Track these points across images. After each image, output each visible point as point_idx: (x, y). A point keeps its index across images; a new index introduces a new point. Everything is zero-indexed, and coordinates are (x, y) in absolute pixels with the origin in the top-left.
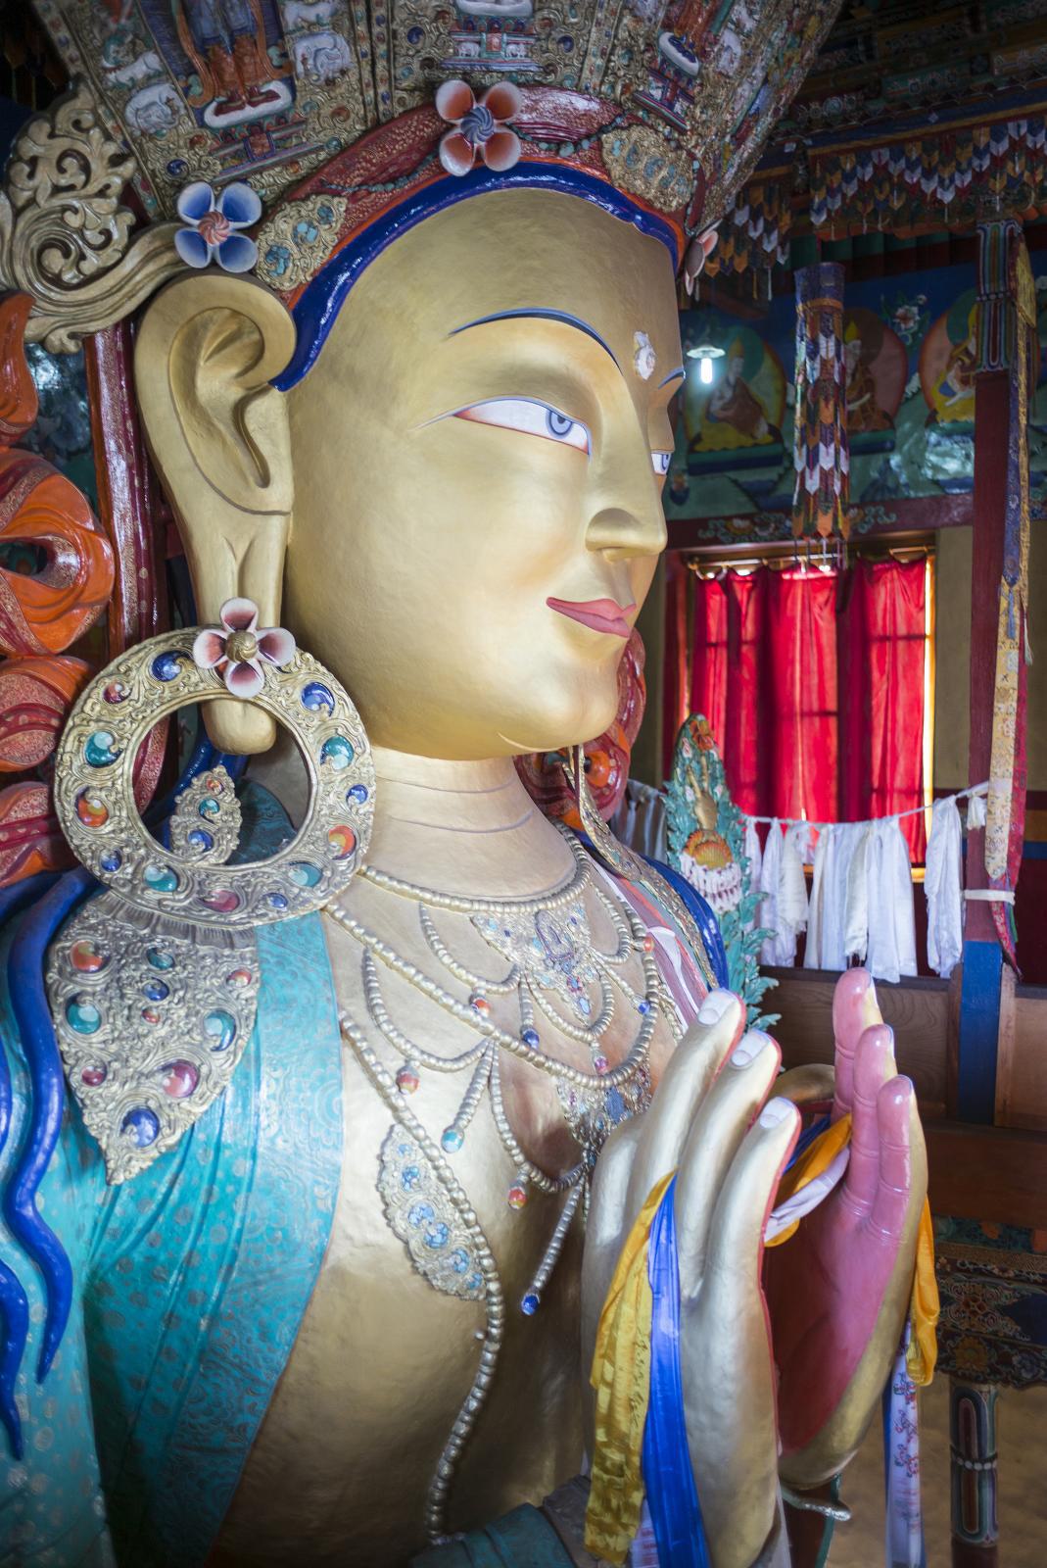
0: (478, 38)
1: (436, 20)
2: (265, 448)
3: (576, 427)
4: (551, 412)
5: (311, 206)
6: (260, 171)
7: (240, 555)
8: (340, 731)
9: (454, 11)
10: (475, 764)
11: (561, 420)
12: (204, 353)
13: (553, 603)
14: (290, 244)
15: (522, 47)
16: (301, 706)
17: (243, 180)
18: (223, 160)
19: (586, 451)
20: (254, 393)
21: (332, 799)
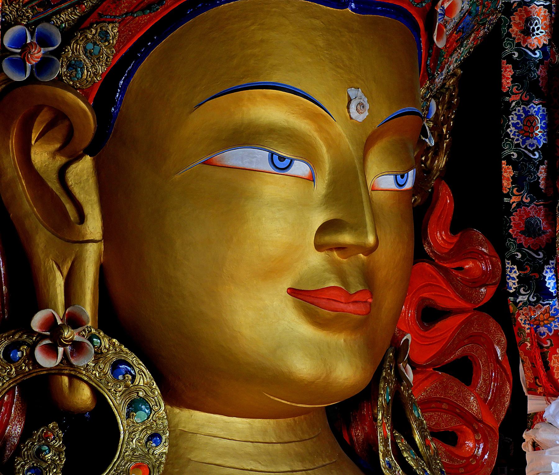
2: (81, 196)
3: (296, 163)
4: (272, 154)
5: (94, 31)
6: (59, 12)
7: (65, 272)
8: (141, 394)
10: (272, 421)
11: (282, 159)
12: (34, 136)
13: (293, 292)
14: (83, 56)
17: (48, 19)
18: (32, 8)
19: (312, 179)
20: (75, 158)
21: (134, 444)
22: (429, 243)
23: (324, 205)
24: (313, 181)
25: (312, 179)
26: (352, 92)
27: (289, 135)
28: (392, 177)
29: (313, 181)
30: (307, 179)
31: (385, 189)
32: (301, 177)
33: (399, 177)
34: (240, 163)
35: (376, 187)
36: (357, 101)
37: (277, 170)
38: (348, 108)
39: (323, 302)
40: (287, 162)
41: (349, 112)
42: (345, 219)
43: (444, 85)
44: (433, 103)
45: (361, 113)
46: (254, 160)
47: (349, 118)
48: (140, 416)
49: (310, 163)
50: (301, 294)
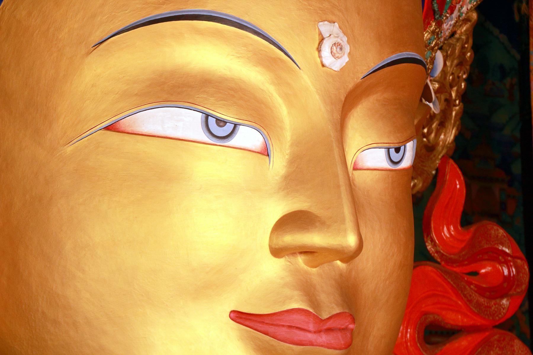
3: (241, 129)
4: (207, 116)
11: (221, 122)
19: (265, 152)
22: (432, 240)
23: (283, 191)
24: (268, 155)
25: (265, 152)
26: (325, 28)
27: (231, 89)
28: (382, 152)
29: (268, 155)
30: (258, 153)
31: (373, 168)
32: (249, 149)
33: (392, 151)
35: (360, 165)
36: (333, 40)
37: (214, 139)
38: (319, 50)
39: (283, 332)
40: (229, 128)
41: (320, 57)
42: (315, 210)
43: (453, 34)
44: (439, 56)
45: (338, 58)
47: (320, 65)
49: (263, 130)
50: (249, 319)
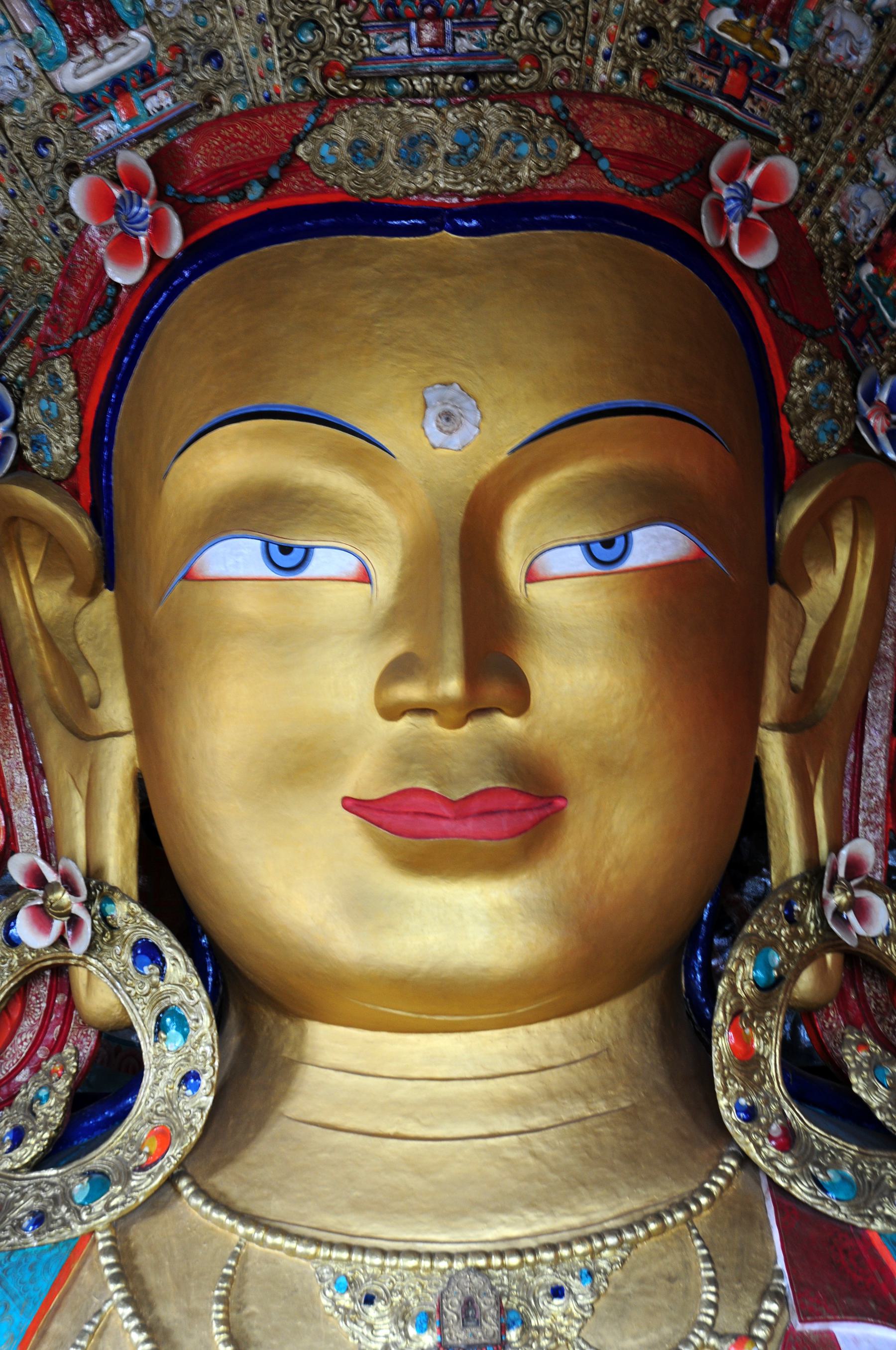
0: (105, 114)
1: (53, 116)
4: (267, 544)
7: (84, 788)
9: (66, 101)
11: (286, 550)
13: (352, 805)
15: (162, 94)
16: (132, 970)
28: (577, 552)
29: (370, 582)
34: (223, 569)
35: (541, 573)
36: (440, 409)
37: (281, 572)
38: (423, 428)
39: (403, 821)
45: (450, 433)
46: (240, 559)
47: (431, 447)
48: (174, 1039)
